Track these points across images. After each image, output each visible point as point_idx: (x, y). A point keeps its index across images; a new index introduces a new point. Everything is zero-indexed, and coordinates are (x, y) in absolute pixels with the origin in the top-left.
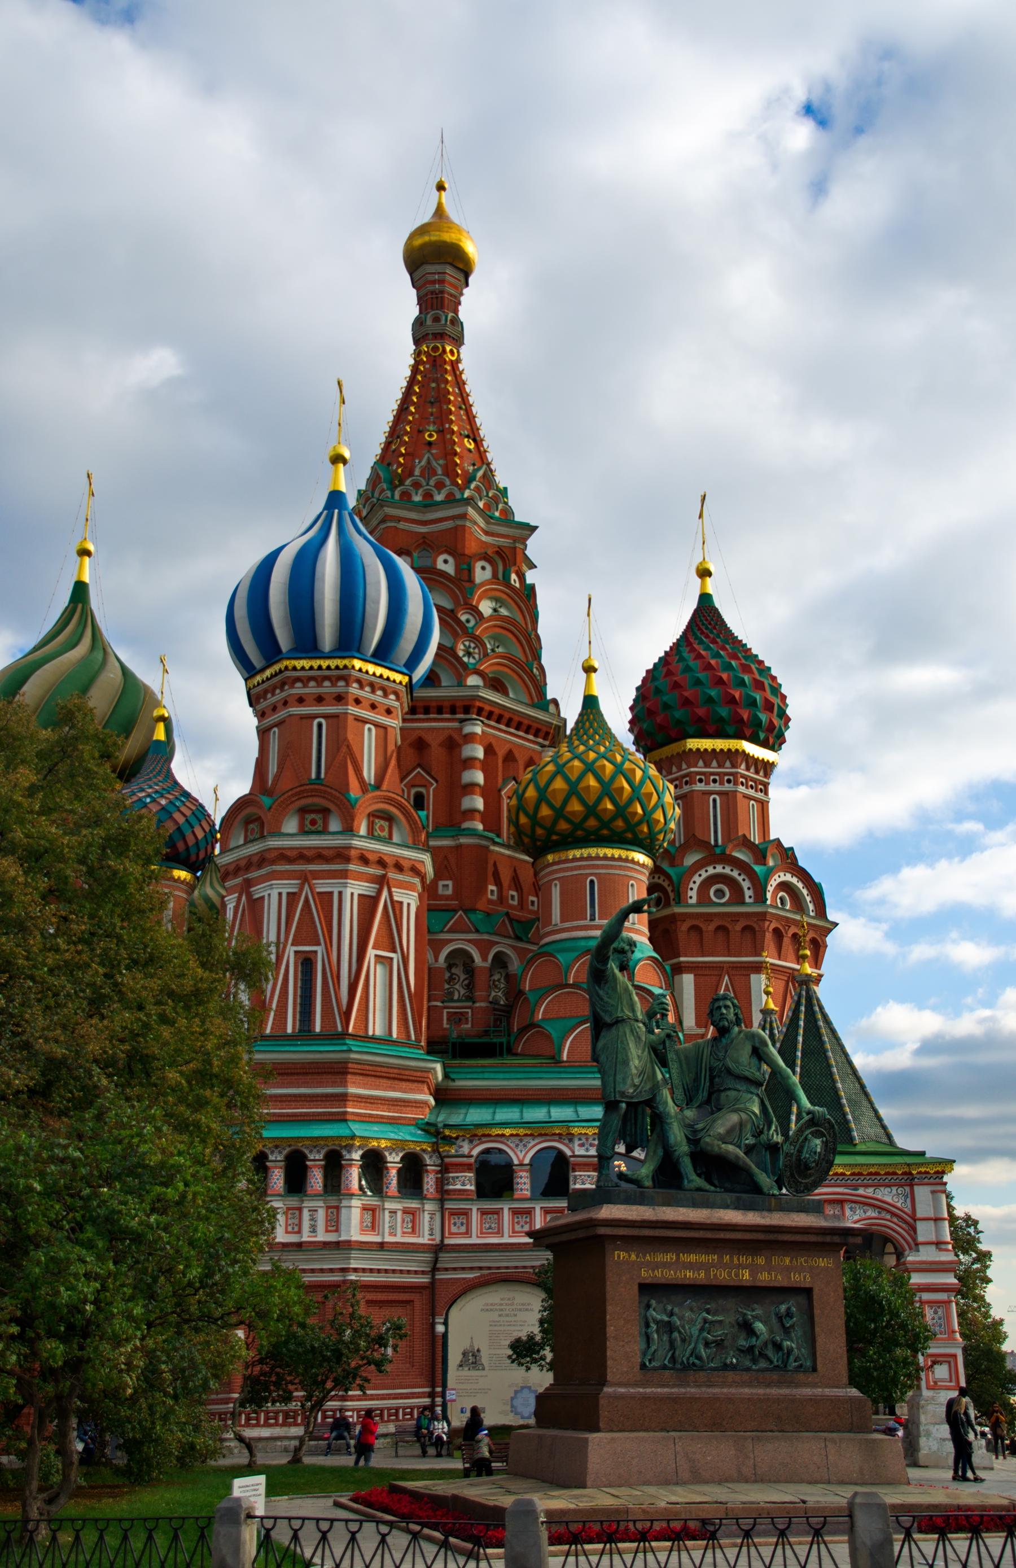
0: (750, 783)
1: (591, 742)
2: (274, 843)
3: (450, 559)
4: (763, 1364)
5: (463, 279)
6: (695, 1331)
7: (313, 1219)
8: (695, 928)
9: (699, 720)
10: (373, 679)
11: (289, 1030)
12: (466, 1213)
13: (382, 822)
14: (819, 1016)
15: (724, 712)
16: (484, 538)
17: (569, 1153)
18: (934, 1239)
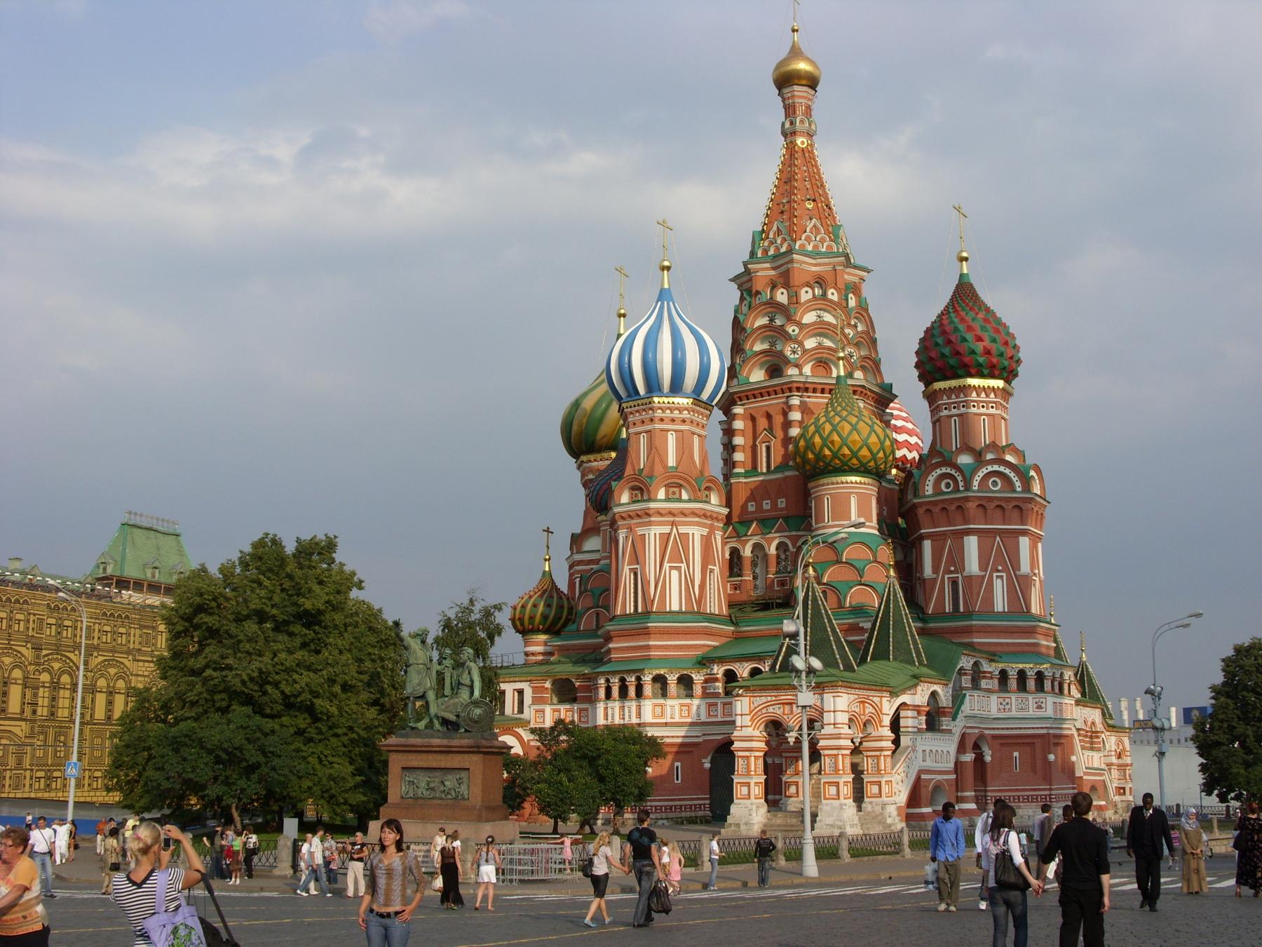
0: (981, 404)
1: (830, 409)
2: (616, 510)
3: (785, 291)
4: (450, 797)
5: (810, 90)
6: (423, 784)
7: (629, 712)
8: (928, 510)
9: (940, 369)
10: (669, 405)
11: (628, 612)
12: (716, 704)
13: (674, 489)
14: (810, 598)
15: (953, 361)
16: (814, 269)
17: (763, 670)
18: (832, 722)
